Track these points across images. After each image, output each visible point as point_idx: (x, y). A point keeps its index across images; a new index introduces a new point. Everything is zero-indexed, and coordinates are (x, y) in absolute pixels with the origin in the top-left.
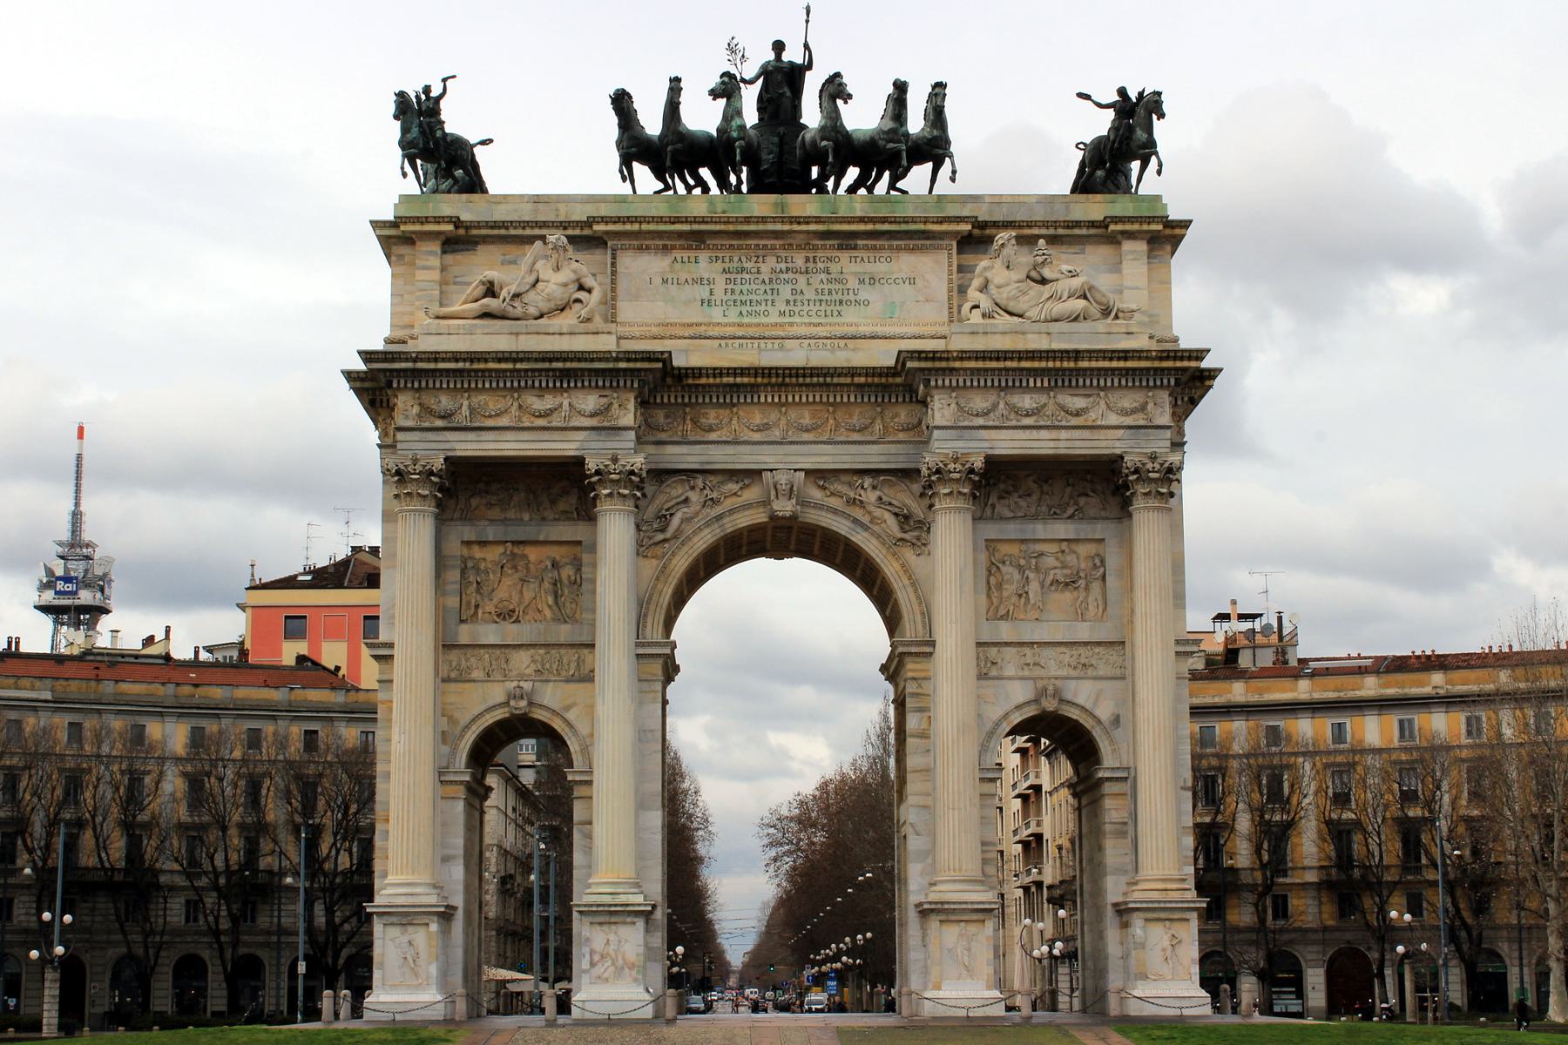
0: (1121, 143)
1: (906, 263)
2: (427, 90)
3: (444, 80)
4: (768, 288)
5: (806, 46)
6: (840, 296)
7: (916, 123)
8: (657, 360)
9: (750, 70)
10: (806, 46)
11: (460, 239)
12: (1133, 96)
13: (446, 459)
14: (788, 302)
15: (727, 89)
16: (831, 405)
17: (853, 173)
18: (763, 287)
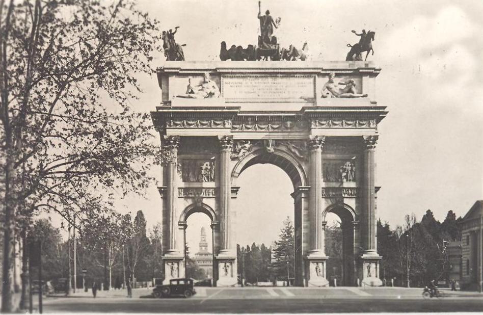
2: (171, 31)
3: (176, 28)
12: (367, 32)
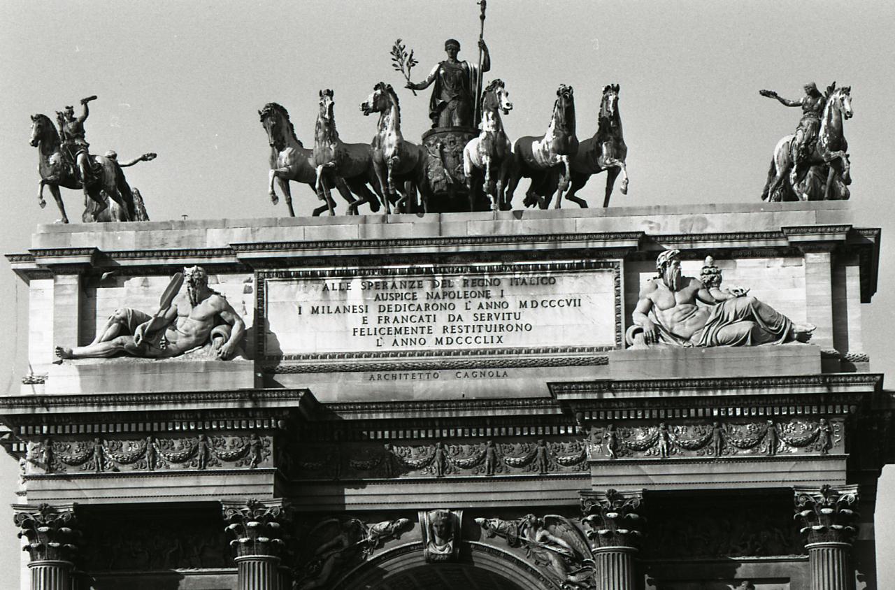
0: (806, 144)
1: (568, 285)
2: (71, 110)
3: (85, 102)
4: (424, 313)
5: (482, 46)
6: (500, 321)
7: (586, 129)
8: (294, 398)
10: (482, 46)
11: (97, 271)
13: (76, 506)
14: (445, 329)
15: (384, 101)
16: (489, 438)
17: (525, 184)
18: (418, 314)
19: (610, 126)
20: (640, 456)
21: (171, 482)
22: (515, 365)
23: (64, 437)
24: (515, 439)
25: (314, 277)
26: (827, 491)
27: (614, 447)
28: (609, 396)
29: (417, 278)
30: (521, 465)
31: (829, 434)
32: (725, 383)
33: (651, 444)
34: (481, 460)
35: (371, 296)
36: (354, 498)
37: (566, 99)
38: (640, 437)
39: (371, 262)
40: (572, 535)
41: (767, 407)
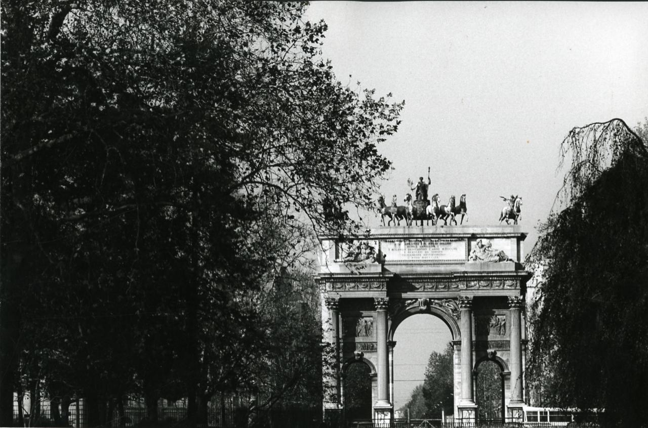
1: (454, 244)
5: (429, 178)
9: (415, 185)
10: (429, 178)
15: (409, 198)
19: (463, 205)
20: (472, 288)
21: (362, 293)
22: (441, 264)
23: (337, 282)
24: (441, 282)
25: (393, 241)
26: (516, 297)
27: (467, 286)
28: (466, 275)
29: (417, 242)
30: (443, 288)
31: (516, 284)
32: (493, 272)
33: (475, 285)
34: (433, 287)
35: (406, 246)
36: (404, 295)
37: (454, 199)
38: (473, 283)
39: (407, 238)
40: (455, 304)
41: (502, 278)
